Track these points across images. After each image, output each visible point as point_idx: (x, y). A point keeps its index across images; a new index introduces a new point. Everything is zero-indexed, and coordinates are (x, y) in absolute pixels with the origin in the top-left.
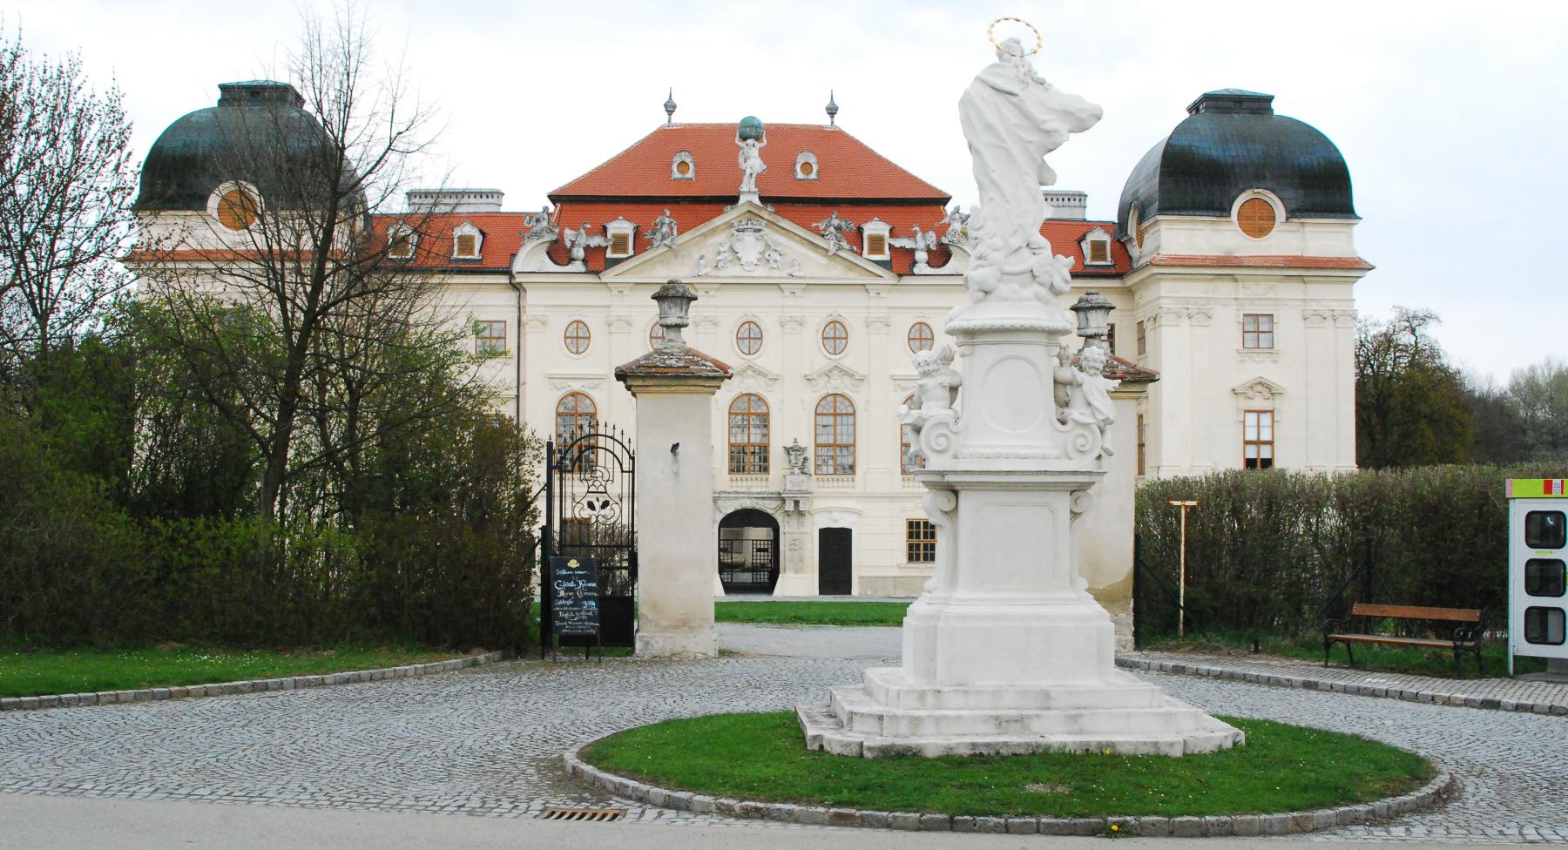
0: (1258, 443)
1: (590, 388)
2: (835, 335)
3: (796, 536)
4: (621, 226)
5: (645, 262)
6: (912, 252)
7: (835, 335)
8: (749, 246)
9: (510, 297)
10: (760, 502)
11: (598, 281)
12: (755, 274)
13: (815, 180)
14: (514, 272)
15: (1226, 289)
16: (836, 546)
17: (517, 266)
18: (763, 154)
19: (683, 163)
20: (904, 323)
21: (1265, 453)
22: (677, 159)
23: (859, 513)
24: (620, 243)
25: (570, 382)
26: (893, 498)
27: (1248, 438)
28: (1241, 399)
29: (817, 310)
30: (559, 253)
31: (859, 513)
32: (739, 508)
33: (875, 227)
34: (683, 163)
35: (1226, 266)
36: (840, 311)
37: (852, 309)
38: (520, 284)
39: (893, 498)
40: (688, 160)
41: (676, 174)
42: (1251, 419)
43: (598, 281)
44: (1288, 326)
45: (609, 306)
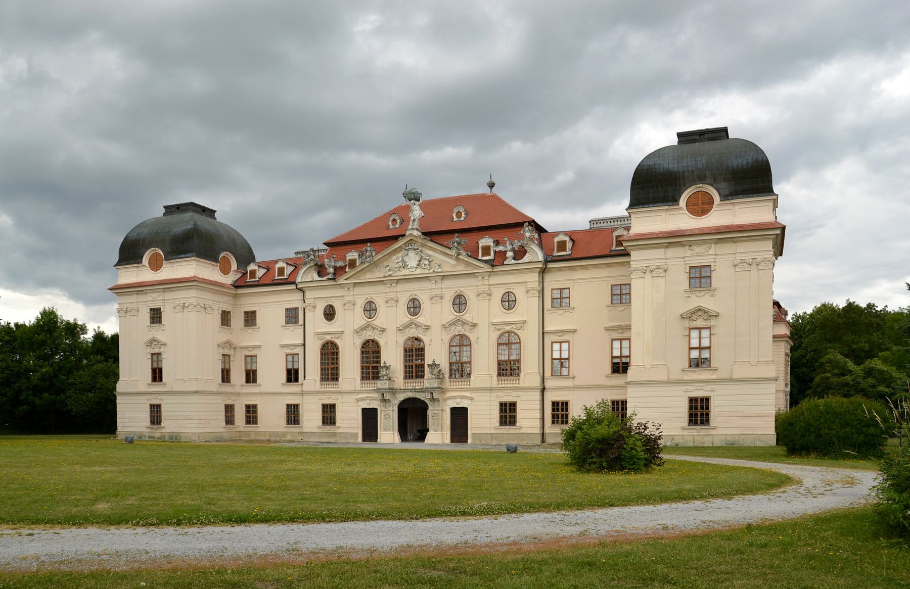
0: (700, 348)
1: (335, 338)
2: (460, 302)
3: (436, 412)
4: (353, 255)
5: (360, 271)
6: (505, 252)
7: (460, 302)
8: (412, 259)
9: (299, 295)
10: (417, 394)
11: (335, 283)
12: (416, 273)
13: (463, 220)
14: (297, 282)
15: (672, 252)
16: (459, 417)
17: (299, 280)
18: (421, 206)
19: (394, 220)
20: (498, 294)
21: (705, 354)
22: (392, 218)
23: (472, 399)
24: (352, 264)
25: (326, 336)
26: (491, 390)
27: (692, 346)
28: (687, 321)
29: (450, 289)
30: (321, 270)
31: (472, 399)
32: (407, 397)
33: (486, 241)
34: (394, 220)
35: (674, 239)
36: (461, 289)
37: (468, 289)
38: (302, 288)
39: (491, 390)
40: (397, 218)
41: (391, 226)
42: (695, 334)
43: (335, 283)
44: (722, 275)
45: (343, 296)
